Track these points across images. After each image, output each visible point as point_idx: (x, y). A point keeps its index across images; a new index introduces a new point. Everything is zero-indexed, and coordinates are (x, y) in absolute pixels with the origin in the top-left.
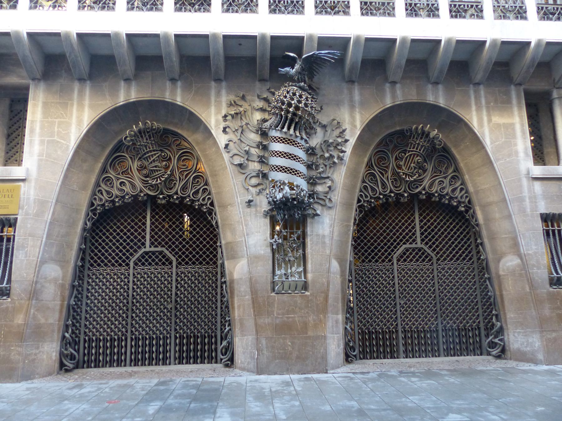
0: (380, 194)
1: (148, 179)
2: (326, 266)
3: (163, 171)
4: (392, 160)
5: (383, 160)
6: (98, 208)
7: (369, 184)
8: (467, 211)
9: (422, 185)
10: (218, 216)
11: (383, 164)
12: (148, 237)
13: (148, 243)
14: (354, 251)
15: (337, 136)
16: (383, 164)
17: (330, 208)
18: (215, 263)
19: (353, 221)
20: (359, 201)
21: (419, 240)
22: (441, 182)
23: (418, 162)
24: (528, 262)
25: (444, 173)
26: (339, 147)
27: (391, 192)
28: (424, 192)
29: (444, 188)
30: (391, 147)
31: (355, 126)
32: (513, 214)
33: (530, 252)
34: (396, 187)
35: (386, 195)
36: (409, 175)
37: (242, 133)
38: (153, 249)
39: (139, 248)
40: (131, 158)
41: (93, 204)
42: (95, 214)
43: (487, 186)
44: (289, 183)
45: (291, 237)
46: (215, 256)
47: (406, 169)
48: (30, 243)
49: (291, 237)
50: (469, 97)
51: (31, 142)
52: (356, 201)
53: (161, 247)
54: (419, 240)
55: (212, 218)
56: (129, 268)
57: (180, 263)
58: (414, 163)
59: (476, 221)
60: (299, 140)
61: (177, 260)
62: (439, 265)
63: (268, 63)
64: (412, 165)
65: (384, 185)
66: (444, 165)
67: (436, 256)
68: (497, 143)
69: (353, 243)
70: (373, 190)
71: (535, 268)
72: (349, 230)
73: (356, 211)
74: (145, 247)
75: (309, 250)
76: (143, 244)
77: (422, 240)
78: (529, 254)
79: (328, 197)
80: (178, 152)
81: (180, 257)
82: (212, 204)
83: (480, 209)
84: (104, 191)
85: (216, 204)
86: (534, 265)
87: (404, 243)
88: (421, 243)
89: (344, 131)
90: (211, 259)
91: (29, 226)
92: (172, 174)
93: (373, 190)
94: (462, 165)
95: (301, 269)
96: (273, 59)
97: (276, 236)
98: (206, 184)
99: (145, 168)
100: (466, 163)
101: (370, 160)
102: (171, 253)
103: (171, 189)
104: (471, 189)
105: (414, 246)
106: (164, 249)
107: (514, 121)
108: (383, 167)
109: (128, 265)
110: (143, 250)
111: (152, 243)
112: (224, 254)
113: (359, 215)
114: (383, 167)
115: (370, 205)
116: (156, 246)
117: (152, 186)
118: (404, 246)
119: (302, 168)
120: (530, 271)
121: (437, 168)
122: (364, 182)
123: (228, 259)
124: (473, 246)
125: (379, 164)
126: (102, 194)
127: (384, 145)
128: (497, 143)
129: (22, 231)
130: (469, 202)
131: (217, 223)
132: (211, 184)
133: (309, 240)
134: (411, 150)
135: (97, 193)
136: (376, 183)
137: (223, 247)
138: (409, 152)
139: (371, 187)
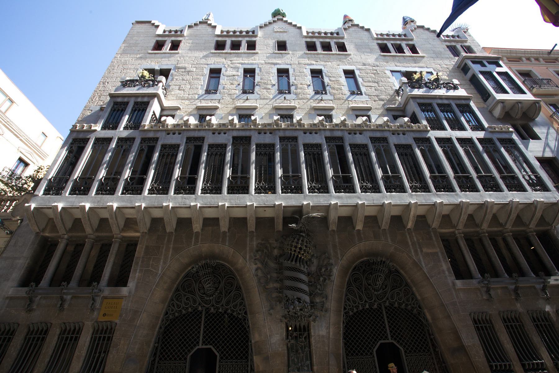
1: (204, 296)
3: (215, 289)
6: (171, 316)
7: (350, 297)
8: (419, 314)
10: (250, 322)
12: (201, 337)
13: (201, 342)
14: (345, 347)
18: (247, 358)
20: (345, 309)
21: (389, 337)
22: (398, 294)
25: (399, 287)
27: (366, 301)
31: (338, 258)
35: (363, 304)
37: (266, 264)
38: (204, 347)
39: (195, 346)
40: (195, 281)
41: (167, 313)
42: (167, 320)
44: (297, 298)
45: (300, 338)
46: (247, 352)
48: (122, 342)
49: (300, 338)
51: (136, 270)
52: (343, 309)
53: (210, 345)
54: (389, 337)
55: (245, 323)
56: (186, 362)
57: (222, 358)
59: (427, 321)
60: (302, 268)
61: (220, 355)
63: (281, 221)
68: (429, 266)
69: (344, 340)
72: (340, 331)
73: (344, 316)
74: (199, 345)
75: (313, 348)
76: (198, 343)
77: (392, 337)
80: (225, 277)
81: (222, 353)
82: (246, 313)
84: (175, 304)
85: (248, 312)
87: (380, 340)
88: (392, 339)
90: (244, 355)
91: (123, 329)
92: (221, 293)
94: (409, 281)
95: (308, 362)
96: (284, 218)
97: (290, 337)
98: (243, 299)
99: (204, 288)
101: (349, 279)
102: (216, 350)
103: (219, 302)
104: (419, 298)
105: (387, 341)
106: (211, 347)
107: (437, 251)
109: (186, 359)
110: (197, 347)
111: (204, 342)
112: (253, 351)
116: (206, 345)
117: (207, 301)
119: (305, 288)
122: (346, 295)
123: (255, 355)
124: (429, 340)
126: (174, 306)
128: (429, 266)
129: (118, 333)
131: (248, 327)
132: (245, 299)
133: (313, 339)
135: (171, 306)
137: (253, 345)
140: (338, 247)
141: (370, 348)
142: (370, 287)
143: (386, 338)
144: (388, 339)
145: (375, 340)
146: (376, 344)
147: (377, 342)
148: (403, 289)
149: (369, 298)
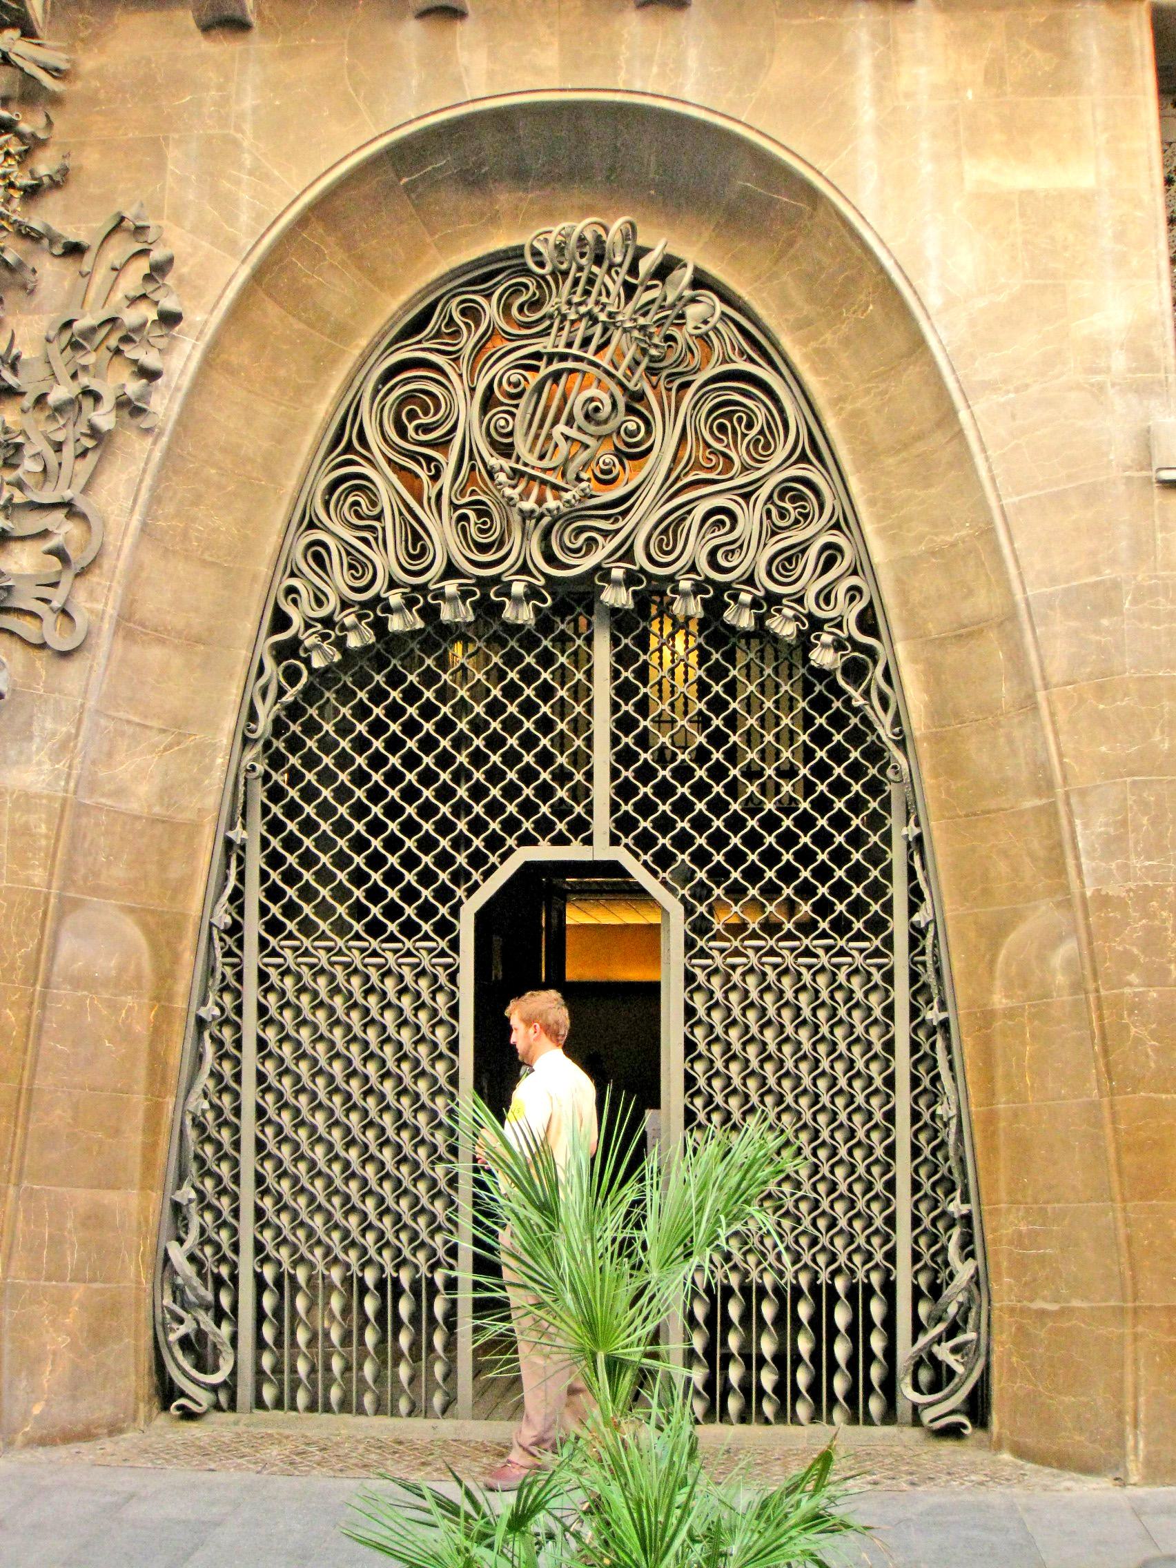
0: (393, 584)
2: (26, 945)
4: (467, 412)
5: (426, 413)
8: (855, 671)
9: (617, 531)
11: (427, 429)
15: (132, 294)
16: (427, 429)
17: (65, 655)
19: (229, 722)
20: (281, 621)
21: (602, 823)
22: (722, 517)
23: (587, 417)
24: (1098, 943)
26: (131, 352)
27: (451, 571)
28: (617, 574)
29: (734, 548)
30: (467, 342)
32: (1039, 682)
33: (1113, 889)
34: (483, 548)
36: (544, 482)
43: (964, 533)
47: (531, 450)
50: (847, 64)
54: (602, 823)
58: (570, 422)
59: (897, 721)
62: (703, 954)
64: (561, 428)
65: (417, 541)
66: (750, 426)
67: (689, 910)
68: (981, 303)
70: (356, 564)
71: (1133, 978)
72: (207, 770)
77: (625, 824)
78: (1104, 901)
79: (56, 604)
83: (914, 660)
86: (1129, 961)
87: (527, 840)
89: (159, 270)
93: (356, 564)
100: (856, 414)
105: (575, 852)
108: (421, 444)
113: (281, 692)
114: (421, 444)
115: (340, 643)
118: (525, 854)
120: (1103, 992)
121: (708, 445)
125: (402, 431)
127: (438, 334)
130: (868, 623)
134: (561, 349)
136: (369, 527)
138: (550, 363)
139: (349, 549)
140: (247, 160)
141: (444, 894)
142: (495, 461)
143: (580, 827)
144: (588, 841)
145: (494, 842)
146: (494, 868)
147: (504, 857)
148: (764, 493)
149: (483, 548)
